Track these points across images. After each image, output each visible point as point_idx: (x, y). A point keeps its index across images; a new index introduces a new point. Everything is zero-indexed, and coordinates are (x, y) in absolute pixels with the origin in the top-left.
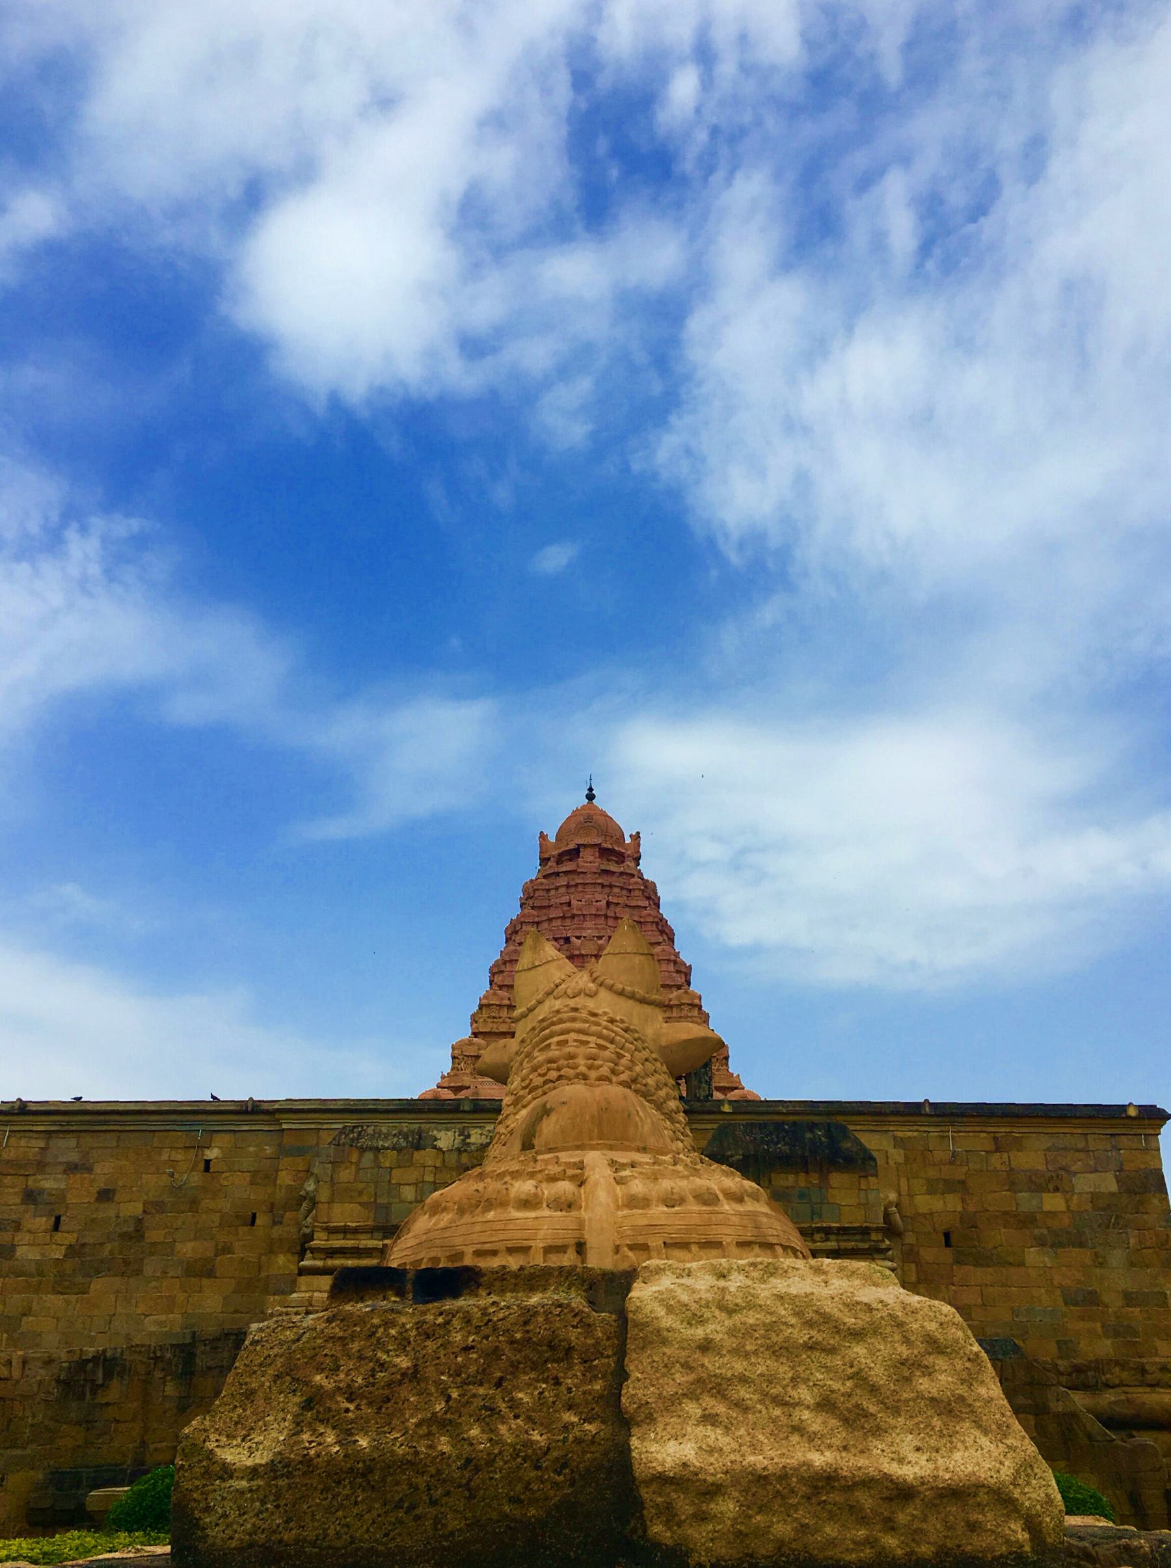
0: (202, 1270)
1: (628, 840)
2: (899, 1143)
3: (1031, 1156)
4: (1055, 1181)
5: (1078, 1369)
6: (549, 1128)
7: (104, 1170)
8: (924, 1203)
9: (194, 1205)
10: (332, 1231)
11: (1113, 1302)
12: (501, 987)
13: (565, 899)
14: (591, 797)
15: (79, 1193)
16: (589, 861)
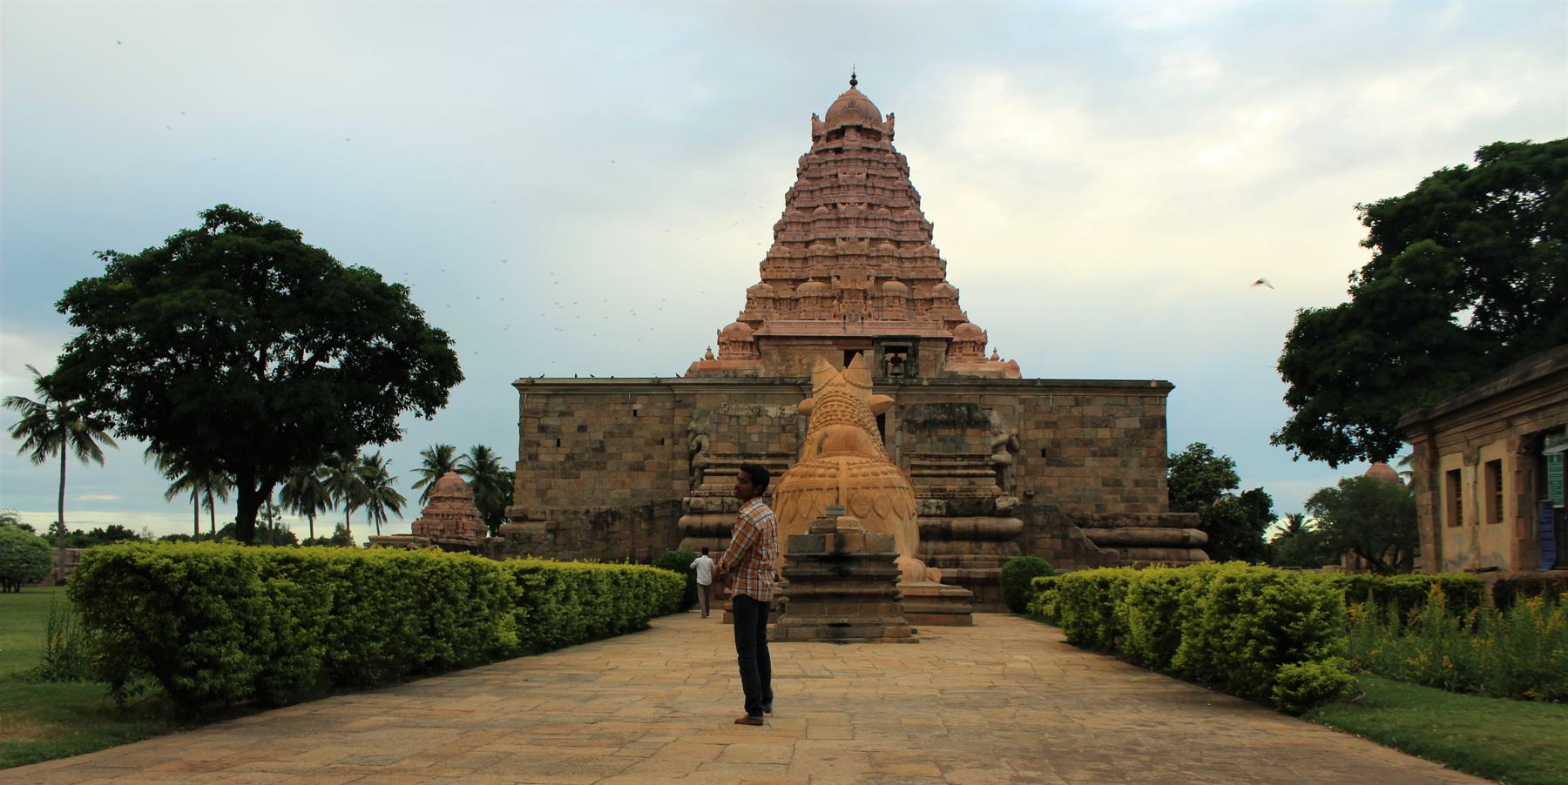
0: (638, 468)
1: (884, 120)
2: (1022, 402)
3: (1095, 409)
4: (1105, 423)
5: (1104, 518)
6: (827, 441)
7: (580, 415)
8: (1034, 434)
9: (630, 434)
10: (719, 455)
11: (1128, 485)
12: (783, 243)
13: (833, 172)
14: (854, 83)
15: (568, 426)
16: (852, 141)
